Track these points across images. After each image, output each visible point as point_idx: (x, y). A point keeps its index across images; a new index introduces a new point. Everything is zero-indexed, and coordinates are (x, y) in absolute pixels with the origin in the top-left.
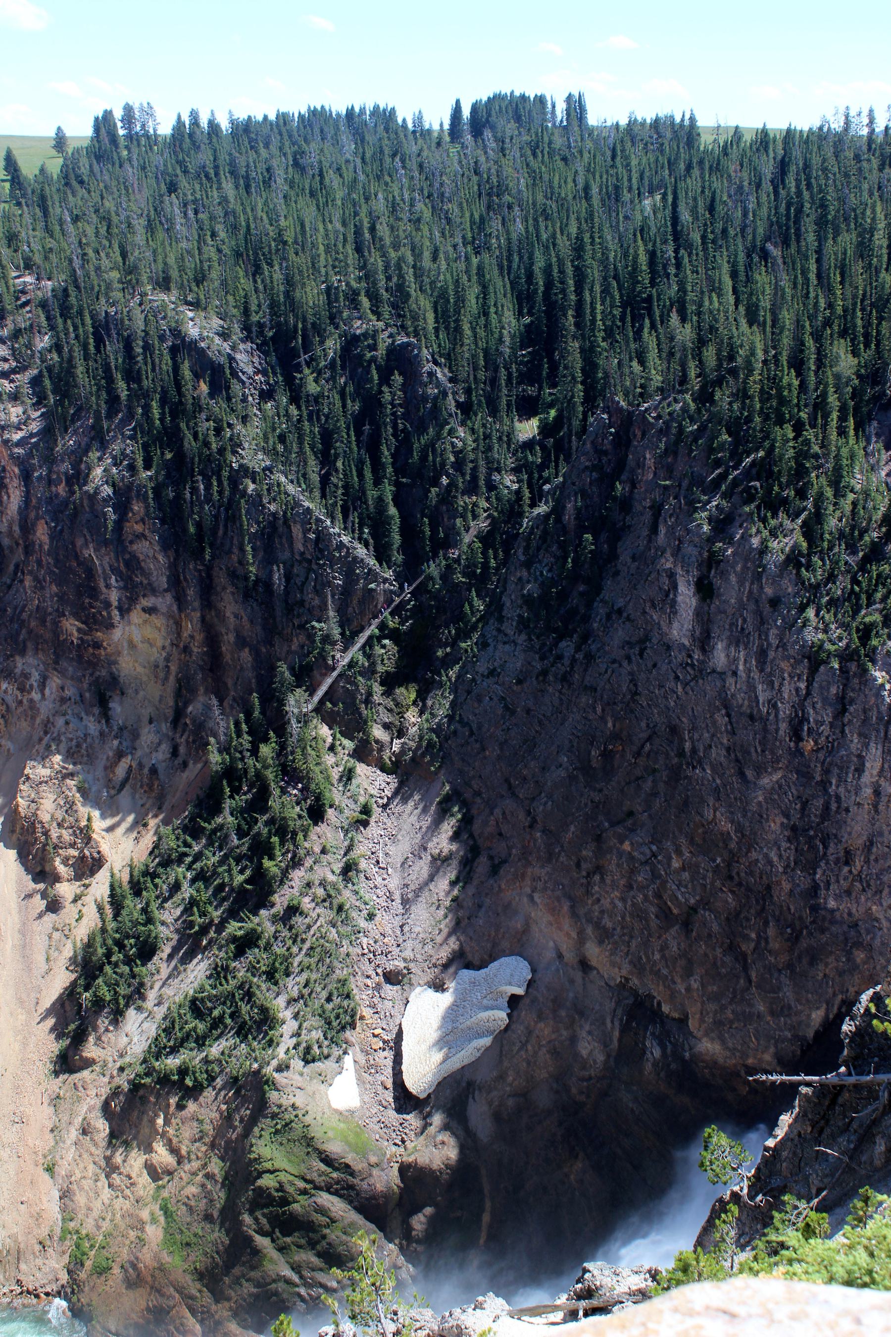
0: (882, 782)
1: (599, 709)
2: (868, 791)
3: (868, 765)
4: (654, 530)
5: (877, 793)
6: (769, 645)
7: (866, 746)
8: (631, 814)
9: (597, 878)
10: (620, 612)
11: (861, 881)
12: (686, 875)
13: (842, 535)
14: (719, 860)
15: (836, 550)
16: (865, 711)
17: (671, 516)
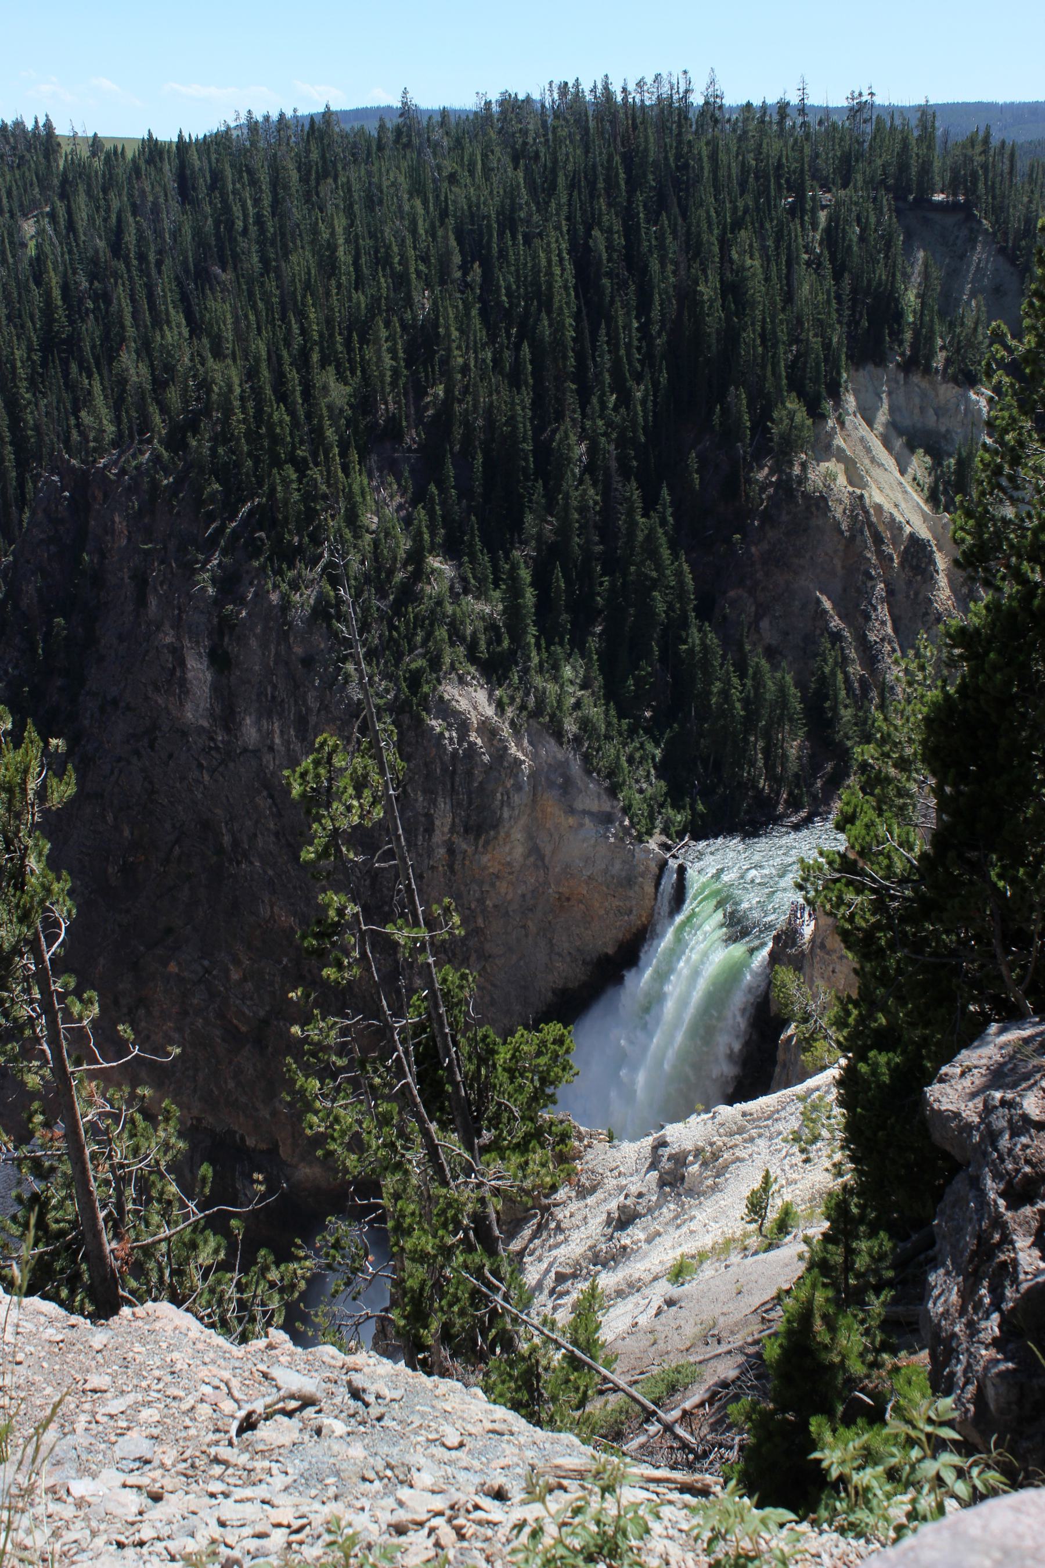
0: (455, 838)
1: (110, 818)
2: (442, 851)
3: (437, 823)
4: (141, 601)
5: (451, 851)
6: (309, 710)
7: (434, 802)
8: (169, 931)
9: (142, 1012)
10: (115, 702)
11: (445, 952)
12: (249, 986)
13: (367, 579)
14: (285, 961)
15: (366, 595)
16: (426, 765)
17: (162, 584)
